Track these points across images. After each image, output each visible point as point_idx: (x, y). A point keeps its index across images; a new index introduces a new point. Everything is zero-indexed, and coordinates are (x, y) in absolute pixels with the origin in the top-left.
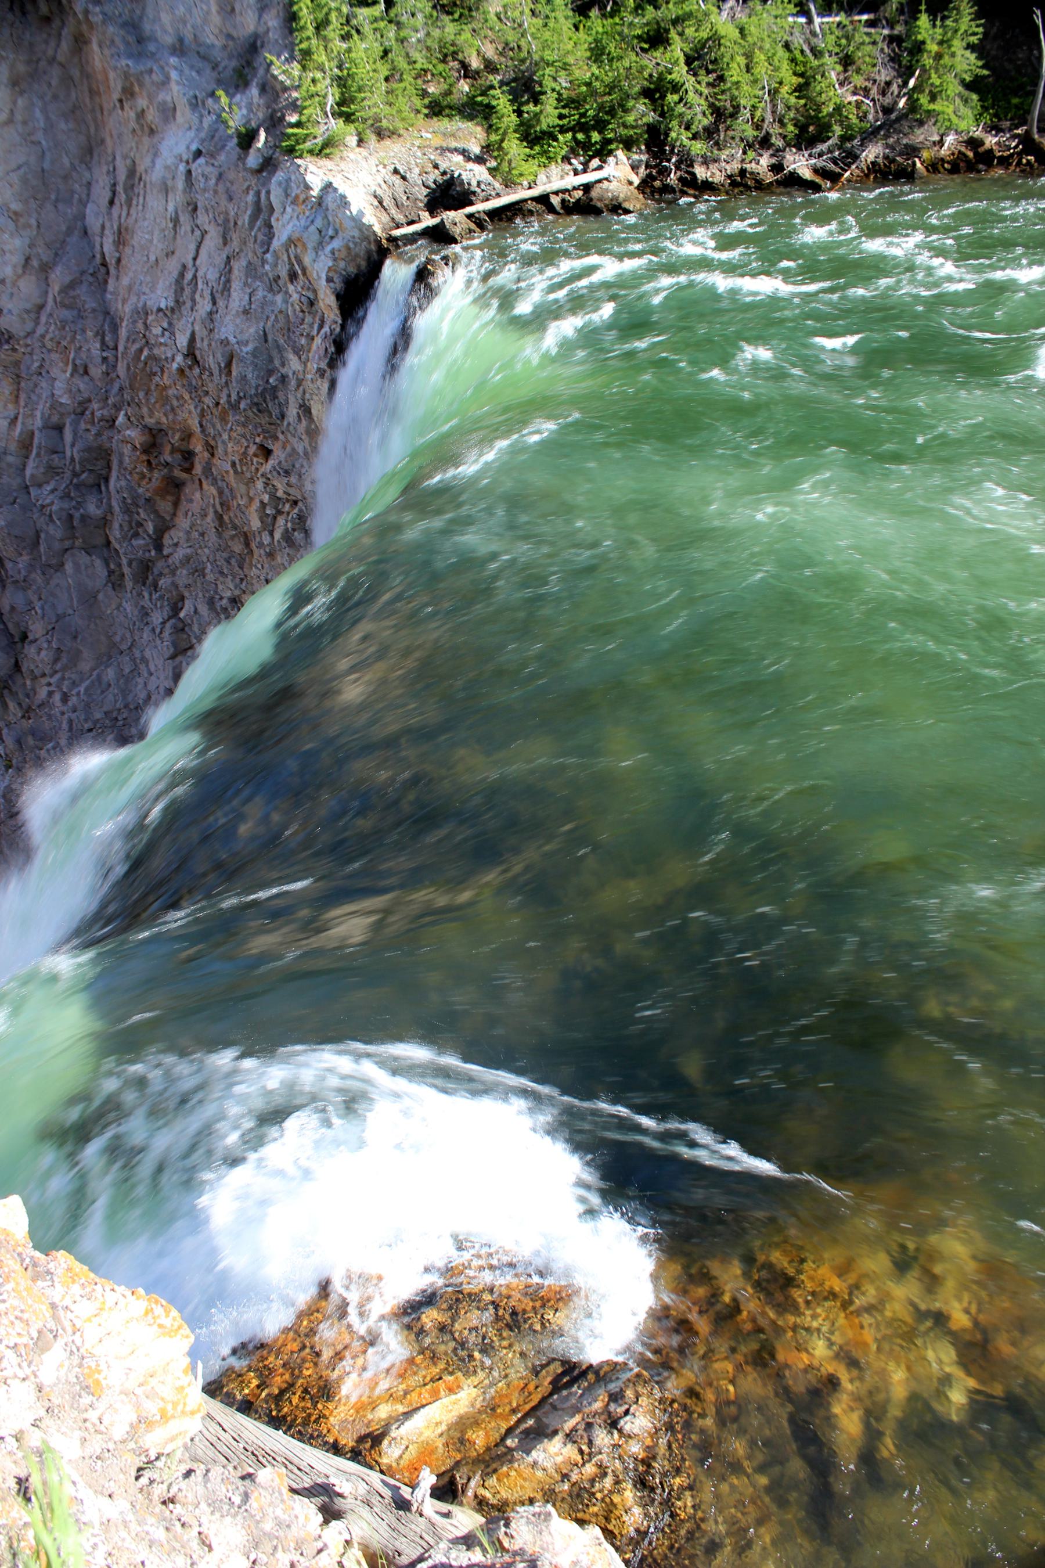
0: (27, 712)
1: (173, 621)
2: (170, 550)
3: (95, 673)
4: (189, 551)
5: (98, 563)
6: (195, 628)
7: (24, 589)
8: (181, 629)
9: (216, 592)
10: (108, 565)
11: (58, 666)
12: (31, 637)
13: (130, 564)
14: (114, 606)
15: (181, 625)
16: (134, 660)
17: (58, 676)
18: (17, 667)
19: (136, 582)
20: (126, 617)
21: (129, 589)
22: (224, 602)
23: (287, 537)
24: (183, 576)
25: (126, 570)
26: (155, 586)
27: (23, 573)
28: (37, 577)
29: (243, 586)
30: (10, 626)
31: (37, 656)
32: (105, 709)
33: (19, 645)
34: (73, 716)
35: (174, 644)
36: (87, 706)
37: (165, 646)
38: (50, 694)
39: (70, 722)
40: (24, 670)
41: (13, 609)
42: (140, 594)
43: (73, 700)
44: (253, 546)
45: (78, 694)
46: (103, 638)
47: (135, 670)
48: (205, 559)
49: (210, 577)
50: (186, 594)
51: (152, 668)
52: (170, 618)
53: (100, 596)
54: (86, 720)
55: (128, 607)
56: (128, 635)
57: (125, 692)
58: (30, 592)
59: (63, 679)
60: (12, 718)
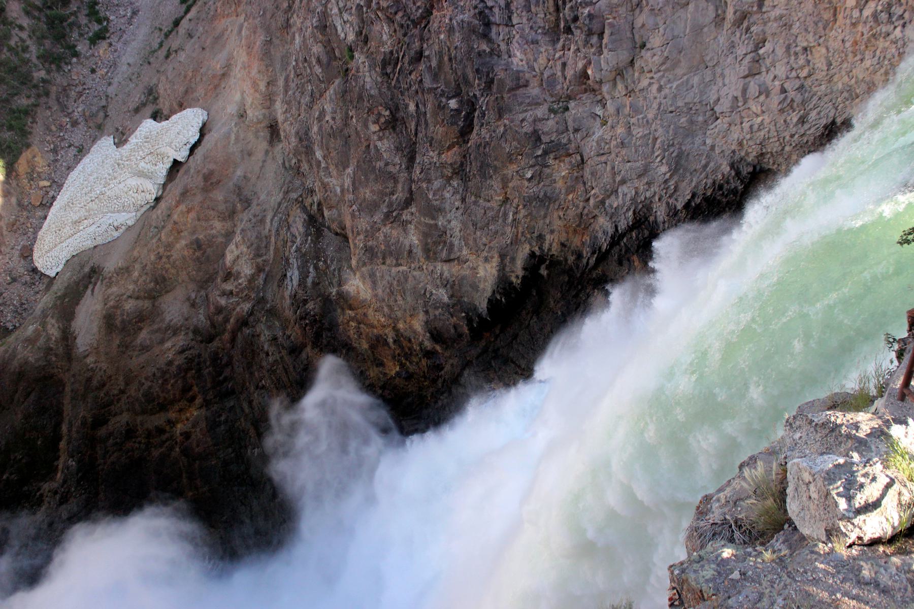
0: (630, 93)
1: (752, 55)
2: (769, 9)
3: (685, 78)
4: (785, 12)
5: (711, 8)
6: (768, 62)
7: (656, 15)
8: (757, 61)
9: (795, 41)
10: (717, 10)
11: (663, 68)
12: (648, 46)
13: (735, 13)
14: (712, 37)
15: (757, 58)
16: (714, 75)
17: (661, 73)
18: (632, 63)
19: (734, 24)
20: (718, 45)
21: (725, 28)
22: (798, 49)
23: (875, 16)
24: (773, 27)
25: (730, 15)
26: (748, 29)
27: (661, 5)
28: (668, 9)
29: (821, 40)
30: (637, 37)
31: (649, 59)
32: (686, 101)
33: (638, 50)
34: (664, 101)
35: (750, 69)
36: (675, 96)
37: (743, 69)
38: (650, 84)
39: (660, 104)
40: (637, 65)
41: (643, 25)
42: (733, 33)
43: (666, 91)
44: (840, 17)
45: (671, 88)
46: (698, 56)
47: (713, 81)
48: (796, 19)
49: (795, 30)
50: (769, 38)
51: (727, 81)
52: (751, 52)
53: (706, 30)
54: (671, 105)
55: (721, 40)
56: (716, 58)
57: (702, 93)
58: (659, 18)
59: (663, 76)
60: (617, 94)
